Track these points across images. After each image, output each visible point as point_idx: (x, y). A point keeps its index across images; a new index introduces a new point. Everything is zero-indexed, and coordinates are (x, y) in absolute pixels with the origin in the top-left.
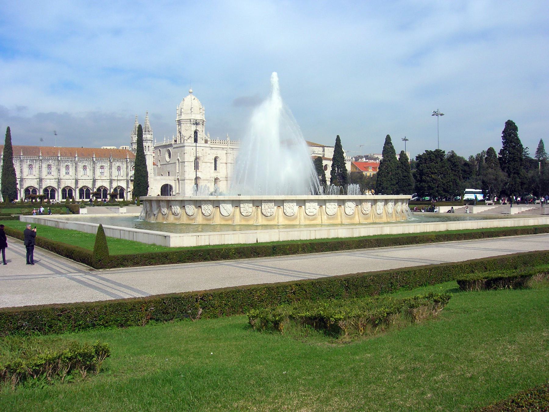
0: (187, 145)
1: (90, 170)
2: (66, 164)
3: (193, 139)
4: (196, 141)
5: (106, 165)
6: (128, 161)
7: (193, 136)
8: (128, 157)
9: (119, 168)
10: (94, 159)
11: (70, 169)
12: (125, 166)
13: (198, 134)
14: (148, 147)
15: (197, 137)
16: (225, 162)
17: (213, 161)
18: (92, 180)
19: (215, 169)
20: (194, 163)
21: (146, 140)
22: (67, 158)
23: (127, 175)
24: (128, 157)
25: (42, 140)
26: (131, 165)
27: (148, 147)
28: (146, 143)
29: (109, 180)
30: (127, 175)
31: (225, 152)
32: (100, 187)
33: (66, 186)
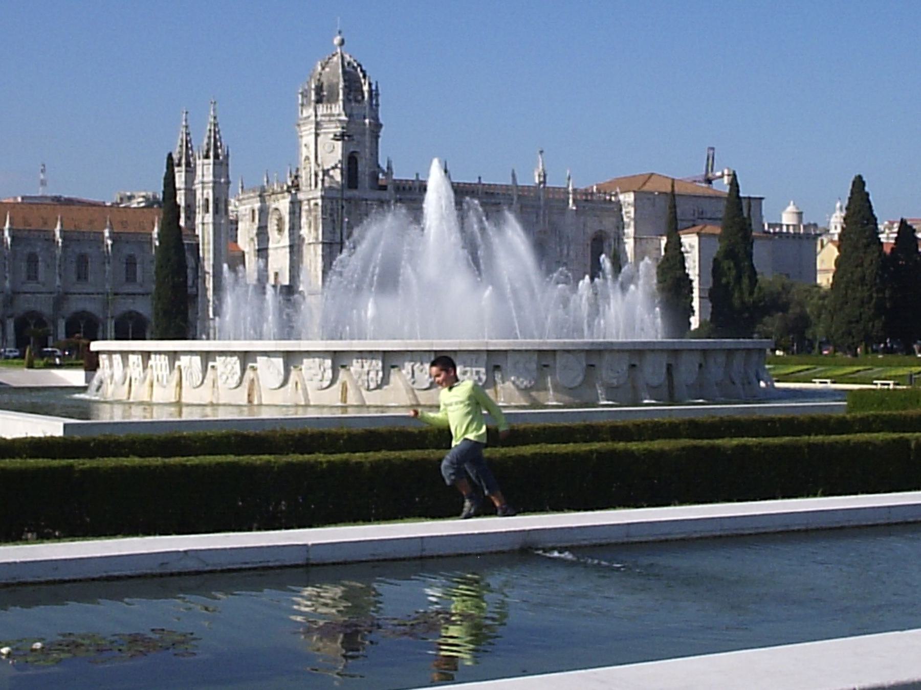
1: (48, 266)
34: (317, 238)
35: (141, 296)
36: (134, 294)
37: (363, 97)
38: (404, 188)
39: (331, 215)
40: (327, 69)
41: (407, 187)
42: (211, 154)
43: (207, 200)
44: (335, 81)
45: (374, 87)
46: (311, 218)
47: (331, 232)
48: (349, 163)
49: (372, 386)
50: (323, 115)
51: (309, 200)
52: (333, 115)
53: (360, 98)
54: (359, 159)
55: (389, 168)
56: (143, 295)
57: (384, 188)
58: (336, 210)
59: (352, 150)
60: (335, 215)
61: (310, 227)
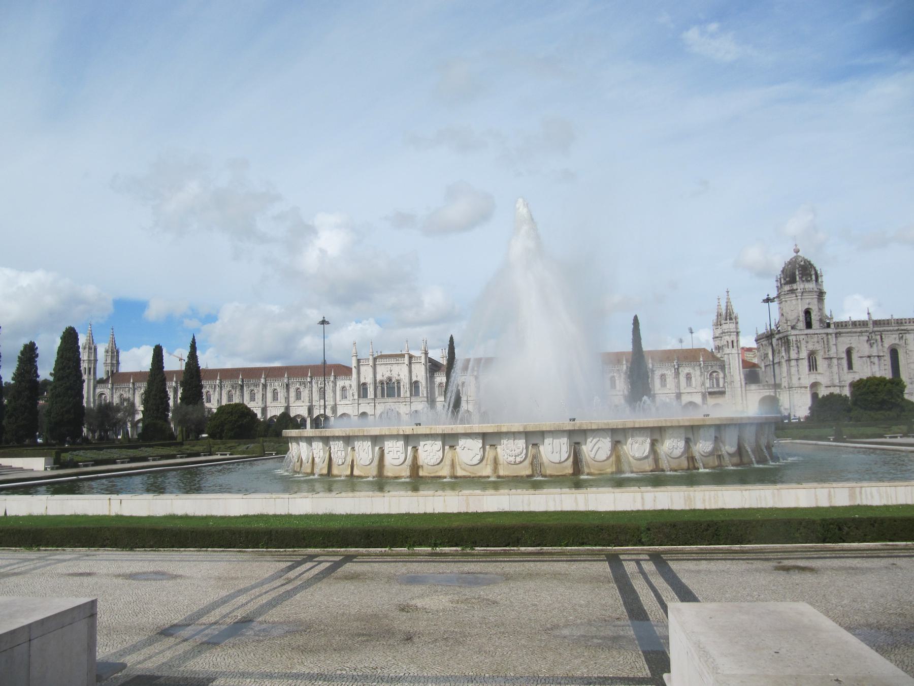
3: (802, 325)
4: (809, 325)
5: (670, 373)
6: (702, 365)
8: (701, 359)
9: (688, 377)
11: (617, 382)
12: (698, 373)
13: (812, 315)
14: (732, 342)
16: (867, 354)
17: (844, 355)
19: (850, 367)
21: (727, 332)
23: (703, 384)
24: (701, 359)
25: (681, 341)
27: (732, 342)
28: (727, 337)
29: (675, 394)
31: (866, 338)
34: (789, 357)
35: (695, 394)
36: (692, 393)
37: (811, 279)
38: (842, 326)
39: (796, 344)
40: (790, 266)
41: (844, 325)
42: (728, 317)
43: (728, 342)
45: (819, 272)
46: (786, 346)
47: (796, 354)
48: (806, 315)
49: (340, 463)
50: (788, 291)
51: (784, 337)
52: (794, 290)
53: (809, 279)
54: (811, 312)
55: (831, 315)
56: (696, 393)
57: (828, 325)
59: (807, 307)
60: (799, 344)
61: (786, 352)
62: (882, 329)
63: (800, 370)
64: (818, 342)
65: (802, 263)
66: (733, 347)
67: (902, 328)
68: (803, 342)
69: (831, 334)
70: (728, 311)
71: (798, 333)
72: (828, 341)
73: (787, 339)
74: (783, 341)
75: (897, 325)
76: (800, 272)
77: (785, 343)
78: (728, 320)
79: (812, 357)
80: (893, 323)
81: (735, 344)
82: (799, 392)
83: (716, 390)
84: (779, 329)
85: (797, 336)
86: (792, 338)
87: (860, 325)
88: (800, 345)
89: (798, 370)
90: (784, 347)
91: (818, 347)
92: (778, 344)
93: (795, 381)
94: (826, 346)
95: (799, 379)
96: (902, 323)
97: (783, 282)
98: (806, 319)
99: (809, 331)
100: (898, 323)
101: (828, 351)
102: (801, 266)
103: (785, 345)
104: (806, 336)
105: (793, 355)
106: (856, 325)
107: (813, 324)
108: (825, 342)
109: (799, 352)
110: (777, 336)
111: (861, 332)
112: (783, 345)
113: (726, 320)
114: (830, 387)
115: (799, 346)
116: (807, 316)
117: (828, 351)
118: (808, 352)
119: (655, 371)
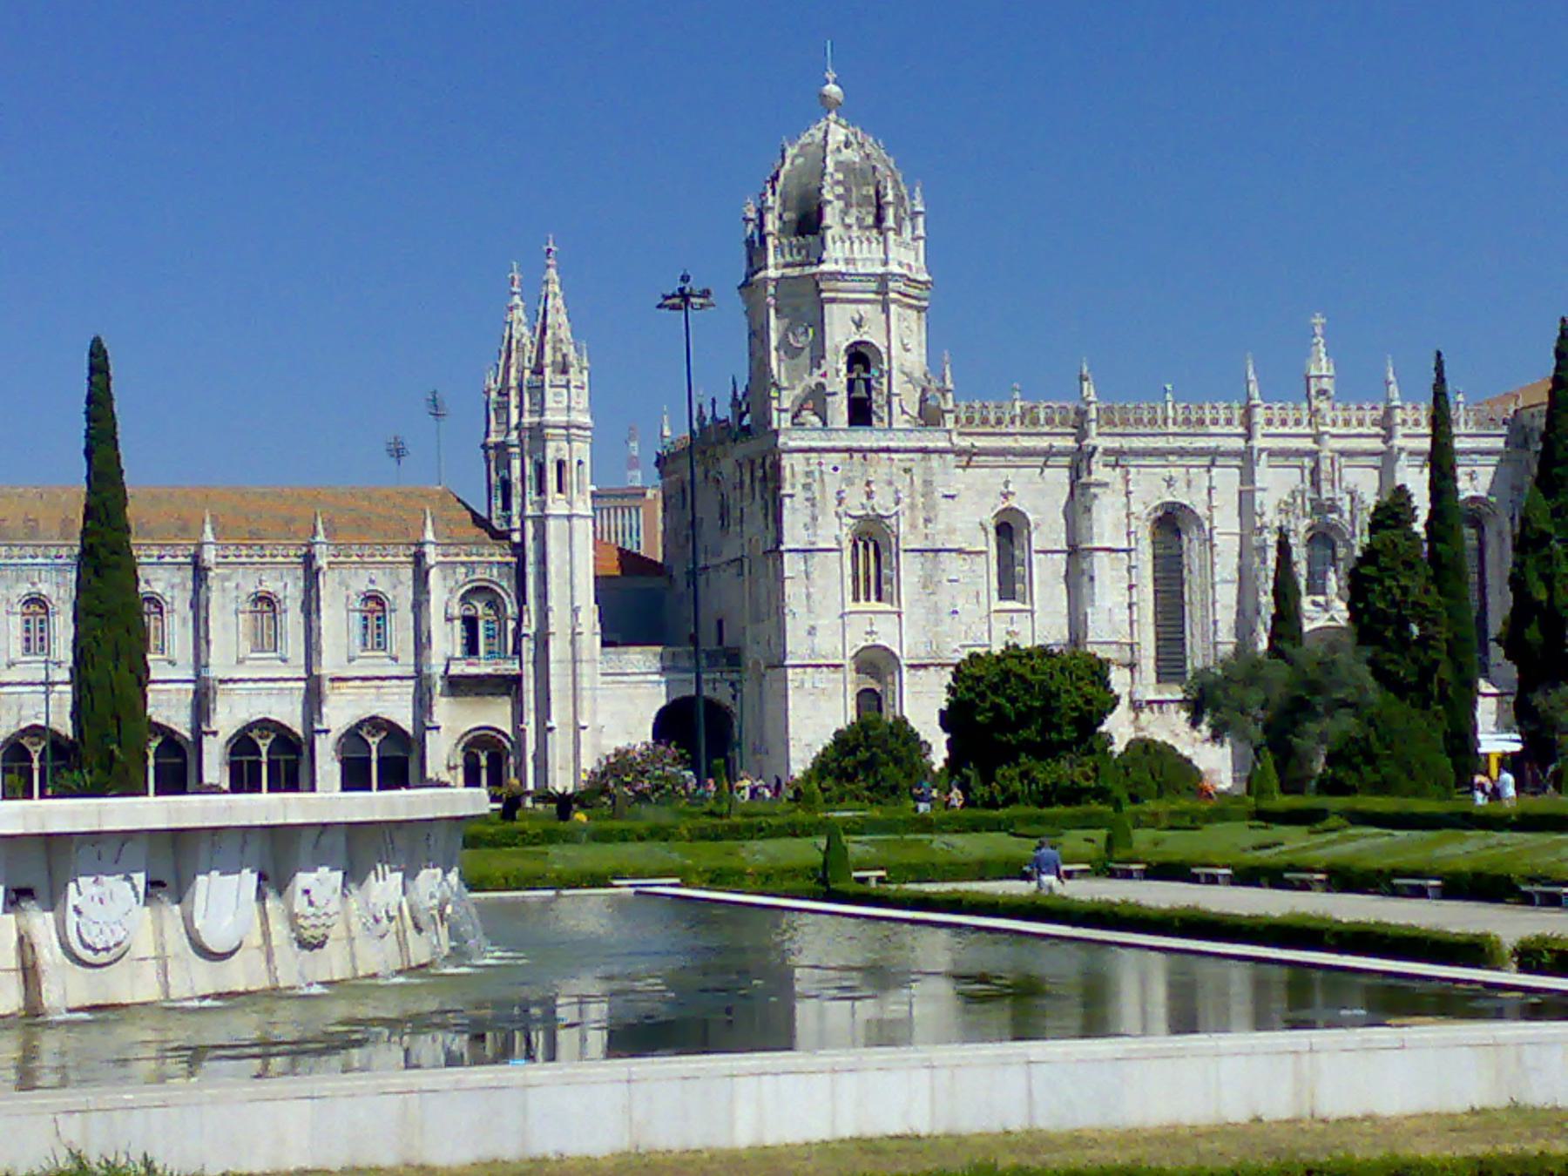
0: (792, 444)
2: (24, 589)
3: (839, 409)
7: (838, 382)
8: (429, 536)
10: (210, 555)
14: (560, 465)
15: (869, 388)
18: (191, 686)
20: (847, 554)
22: (30, 551)
24: (429, 536)
26: (451, 583)
30: (421, 644)
32: (250, 726)
33: (24, 725)
39: (807, 487)
41: (992, 419)
44: (815, 184)
46: (768, 496)
48: (850, 370)
53: (870, 220)
58: (817, 474)
60: (816, 487)
61: (766, 515)
62: (1126, 443)
63: (816, 597)
64: (890, 483)
65: (848, 154)
66: (560, 490)
67: (1201, 443)
68: (833, 483)
69: (941, 452)
70: (549, 332)
71: (814, 444)
72: (927, 483)
73: (777, 467)
74: (759, 473)
75: (1184, 429)
76: (840, 190)
77: (764, 478)
78: (548, 371)
79: (866, 547)
80: (1170, 421)
81: (571, 476)
82: (808, 685)
83: (483, 668)
84: (746, 421)
85: (813, 455)
86: (792, 465)
87: (1050, 421)
88: (823, 492)
89: (808, 596)
90: (762, 497)
91: (883, 503)
92: (742, 483)
93: (796, 645)
94: (920, 500)
95: (812, 631)
96: (1201, 422)
97: (771, 224)
98: (851, 386)
99: (863, 438)
100: (1187, 421)
101: (927, 521)
102: (839, 165)
103: (764, 489)
104: (847, 455)
105: (794, 533)
106: (1035, 422)
107: (874, 407)
108: (918, 481)
109: (814, 518)
110: (741, 450)
111: (1049, 453)
112: (757, 486)
113: (538, 371)
114: (925, 666)
115: (818, 496)
116: (854, 375)
117: (927, 521)
118: (850, 521)
119: (226, 578)
